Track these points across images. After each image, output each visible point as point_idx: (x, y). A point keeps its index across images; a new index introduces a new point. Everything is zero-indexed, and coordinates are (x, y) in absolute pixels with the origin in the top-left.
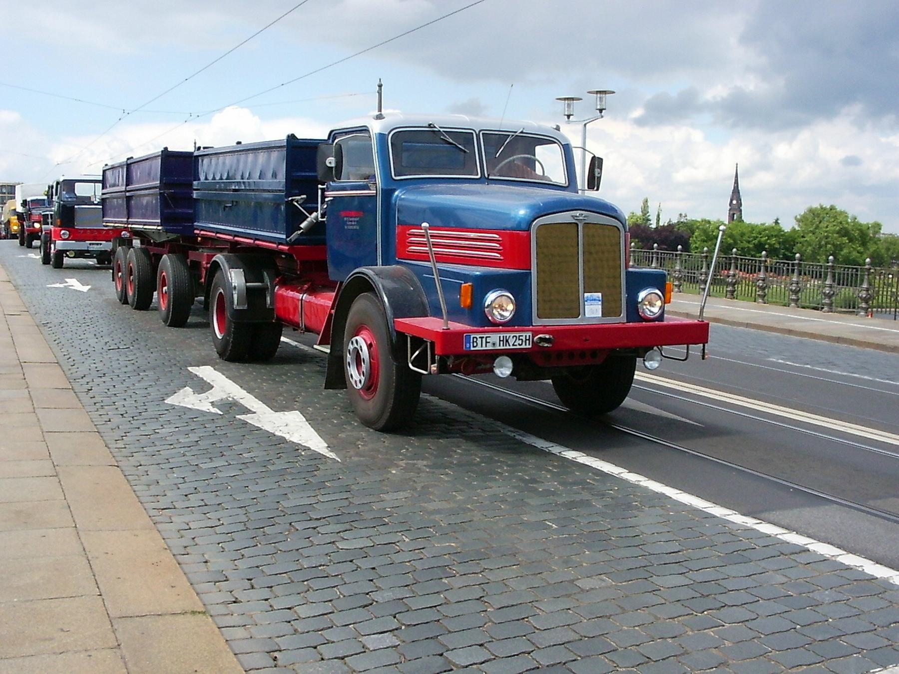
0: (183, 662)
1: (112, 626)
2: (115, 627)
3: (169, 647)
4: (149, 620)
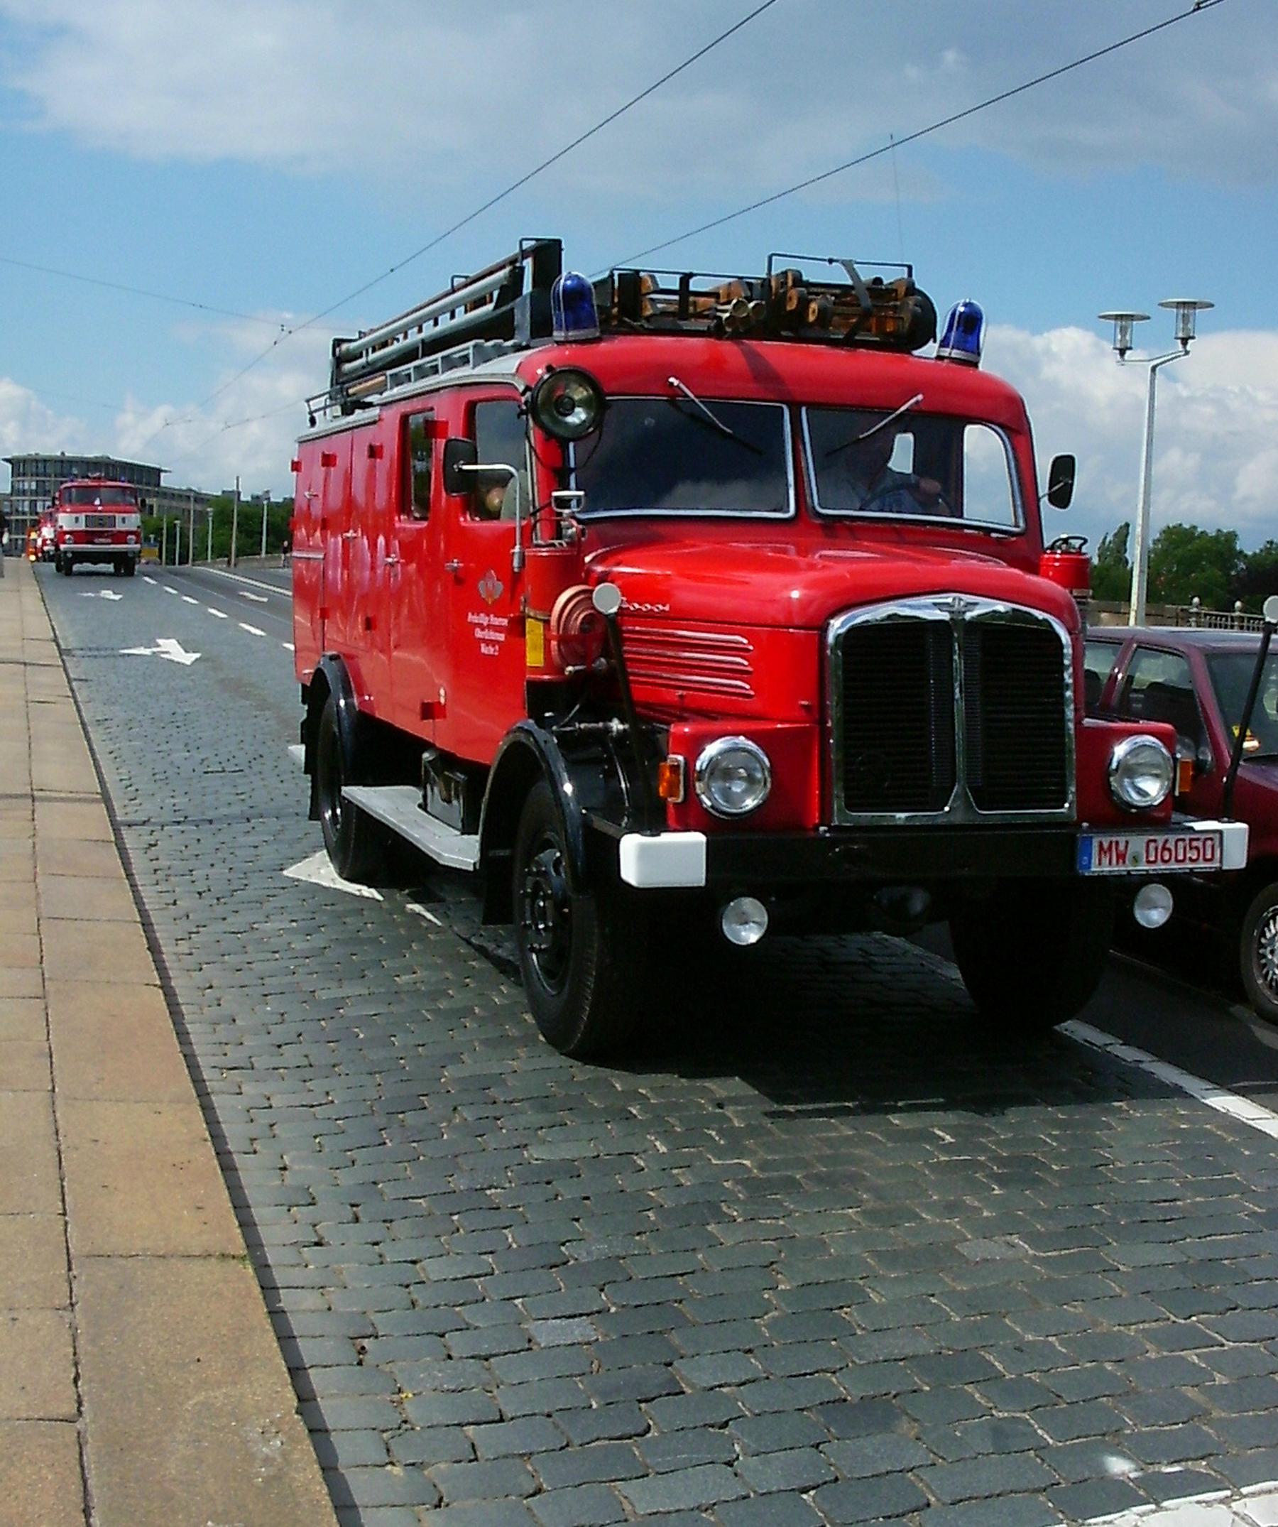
0: (179, 1343)
1: (70, 1269)
2: (75, 1272)
3: (162, 1315)
4: (140, 1264)
